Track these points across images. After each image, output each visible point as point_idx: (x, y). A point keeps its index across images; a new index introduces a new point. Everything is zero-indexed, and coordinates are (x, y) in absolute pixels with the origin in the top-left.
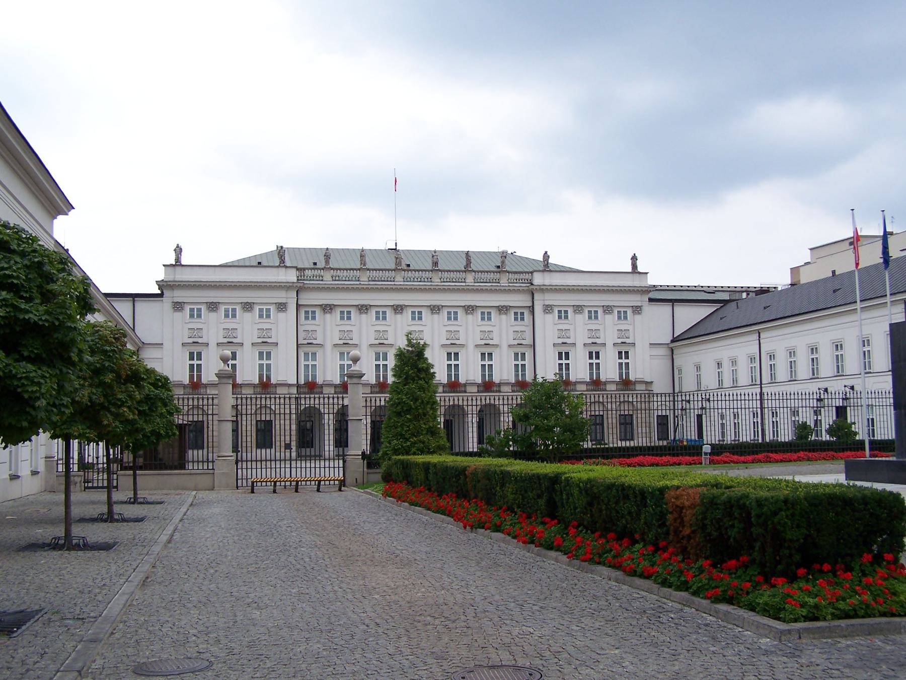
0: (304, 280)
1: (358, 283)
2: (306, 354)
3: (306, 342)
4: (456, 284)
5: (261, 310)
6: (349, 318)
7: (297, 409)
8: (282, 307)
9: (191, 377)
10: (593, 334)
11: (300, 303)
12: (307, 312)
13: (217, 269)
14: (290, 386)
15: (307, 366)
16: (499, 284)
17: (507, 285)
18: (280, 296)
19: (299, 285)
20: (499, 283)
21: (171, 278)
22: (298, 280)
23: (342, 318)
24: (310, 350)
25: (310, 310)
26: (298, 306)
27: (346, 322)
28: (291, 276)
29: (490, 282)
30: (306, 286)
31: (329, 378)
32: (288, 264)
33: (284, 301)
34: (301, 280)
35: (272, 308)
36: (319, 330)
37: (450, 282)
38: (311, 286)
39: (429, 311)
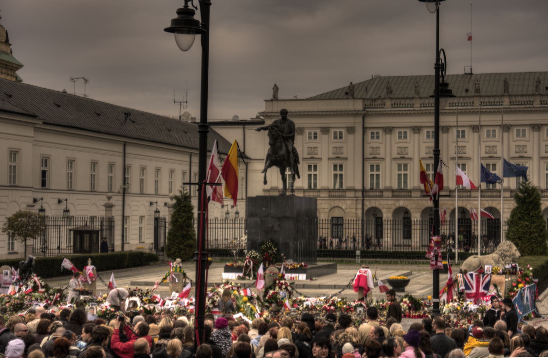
0: (370, 108)
1: (412, 109)
2: (372, 166)
3: (371, 156)
4: (494, 107)
5: (335, 133)
6: (405, 137)
7: (363, 209)
8: (351, 130)
9: (310, 184)
10: (521, 149)
11: (367, 125)
12: (373, 133)
13: (303, 102)
14: (355, 190)
15: (372, 176)
16: (532, 106)
17: (539, 106)
18: (349, 121)
19: (363, 112)
20: (532, 104)
21: (270, 110)
22: (365, 108)
23: (400, 137)
24: (375, 162)
25: (375, 131)
26: (364, 129)
27: (403, 140)
28: (358, 105)
29: (524, 104)
30: (370, 113)
31: (388, 184)
32: (355, 96)
33: (352, 125)
34: (367, 108)
35: (344, 131)
36: (382, 147)
37: (489, 105)
38: (374, 113)
39: (471, 131)
